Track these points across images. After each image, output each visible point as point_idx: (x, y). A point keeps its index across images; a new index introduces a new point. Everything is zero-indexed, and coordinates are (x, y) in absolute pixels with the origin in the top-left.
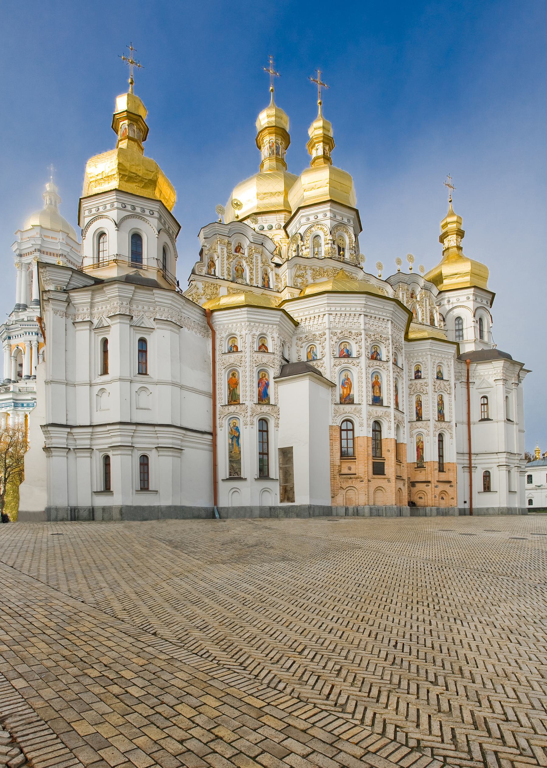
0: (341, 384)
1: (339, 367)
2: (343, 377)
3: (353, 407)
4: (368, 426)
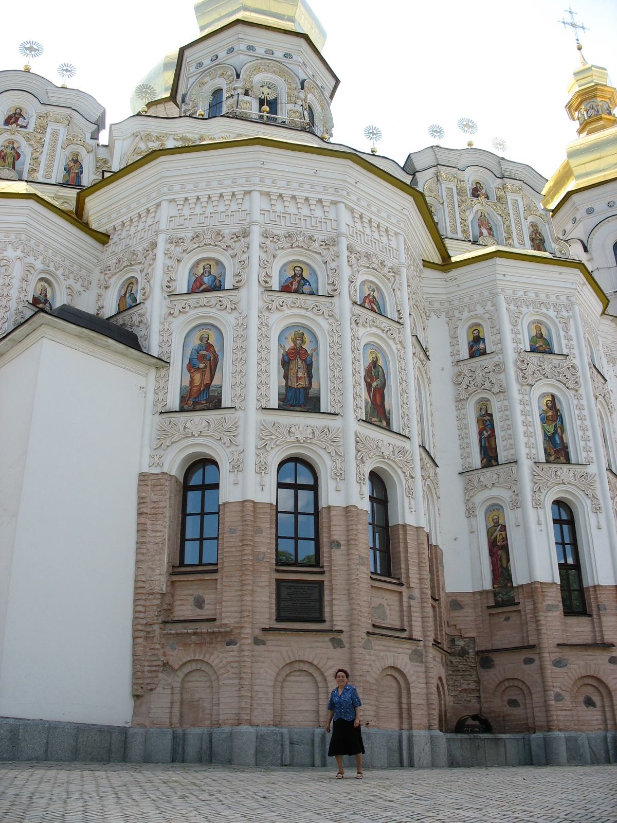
0: (187, 361)
1: (182, 318)
2: (195, 342)
3: (213, 416)
4: (262, 468)
